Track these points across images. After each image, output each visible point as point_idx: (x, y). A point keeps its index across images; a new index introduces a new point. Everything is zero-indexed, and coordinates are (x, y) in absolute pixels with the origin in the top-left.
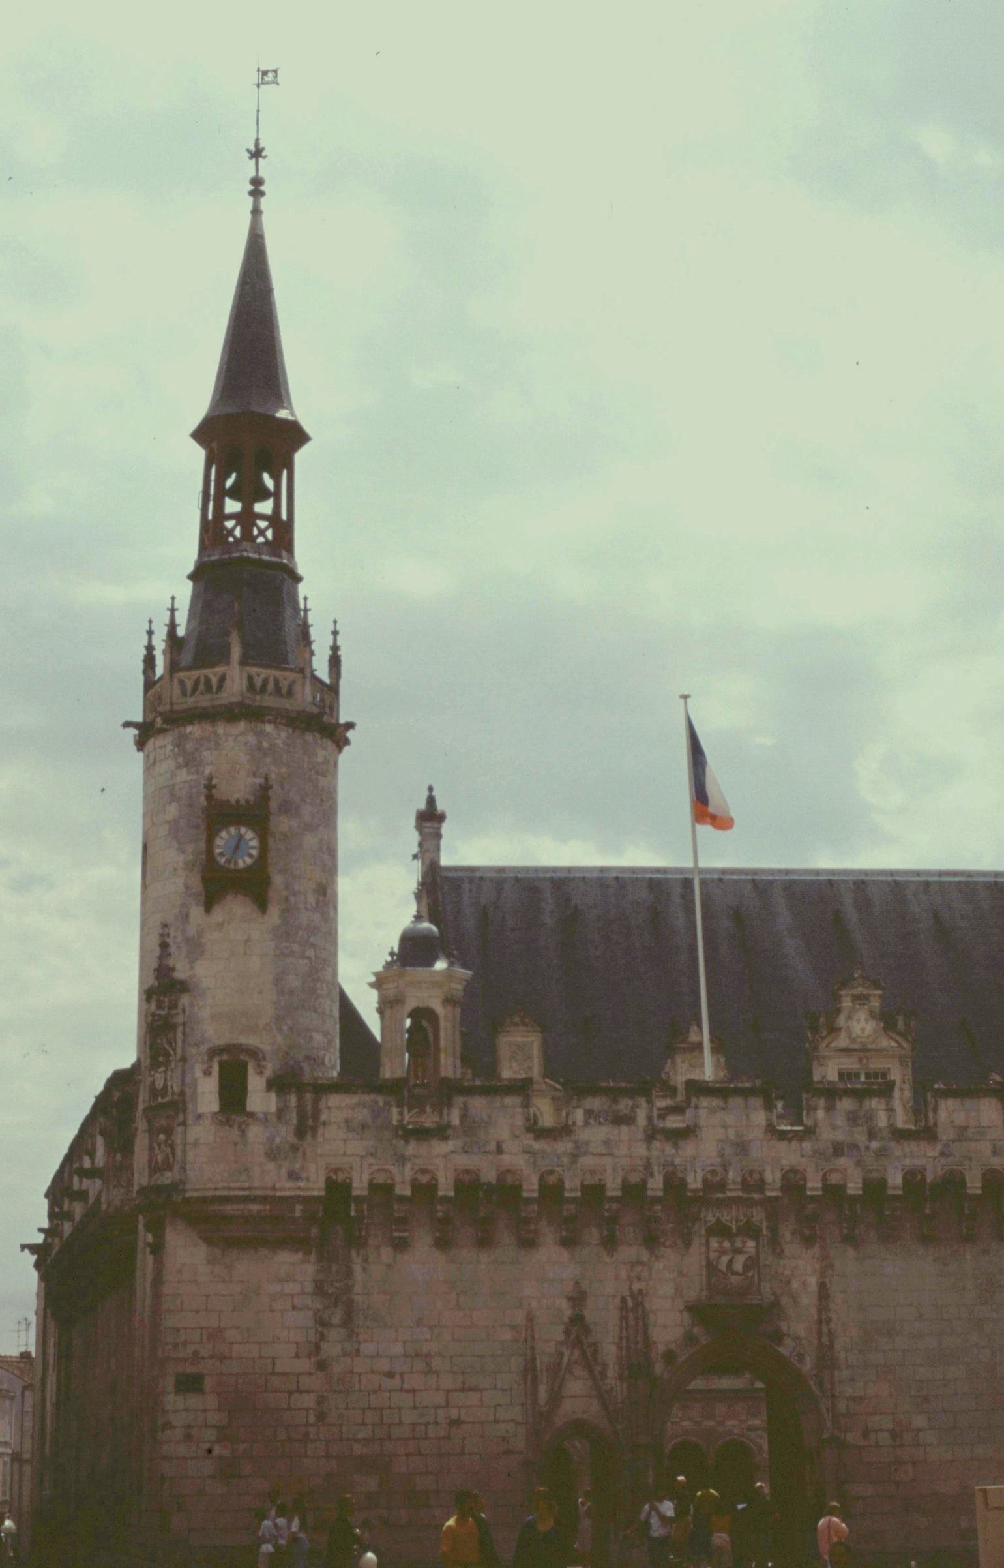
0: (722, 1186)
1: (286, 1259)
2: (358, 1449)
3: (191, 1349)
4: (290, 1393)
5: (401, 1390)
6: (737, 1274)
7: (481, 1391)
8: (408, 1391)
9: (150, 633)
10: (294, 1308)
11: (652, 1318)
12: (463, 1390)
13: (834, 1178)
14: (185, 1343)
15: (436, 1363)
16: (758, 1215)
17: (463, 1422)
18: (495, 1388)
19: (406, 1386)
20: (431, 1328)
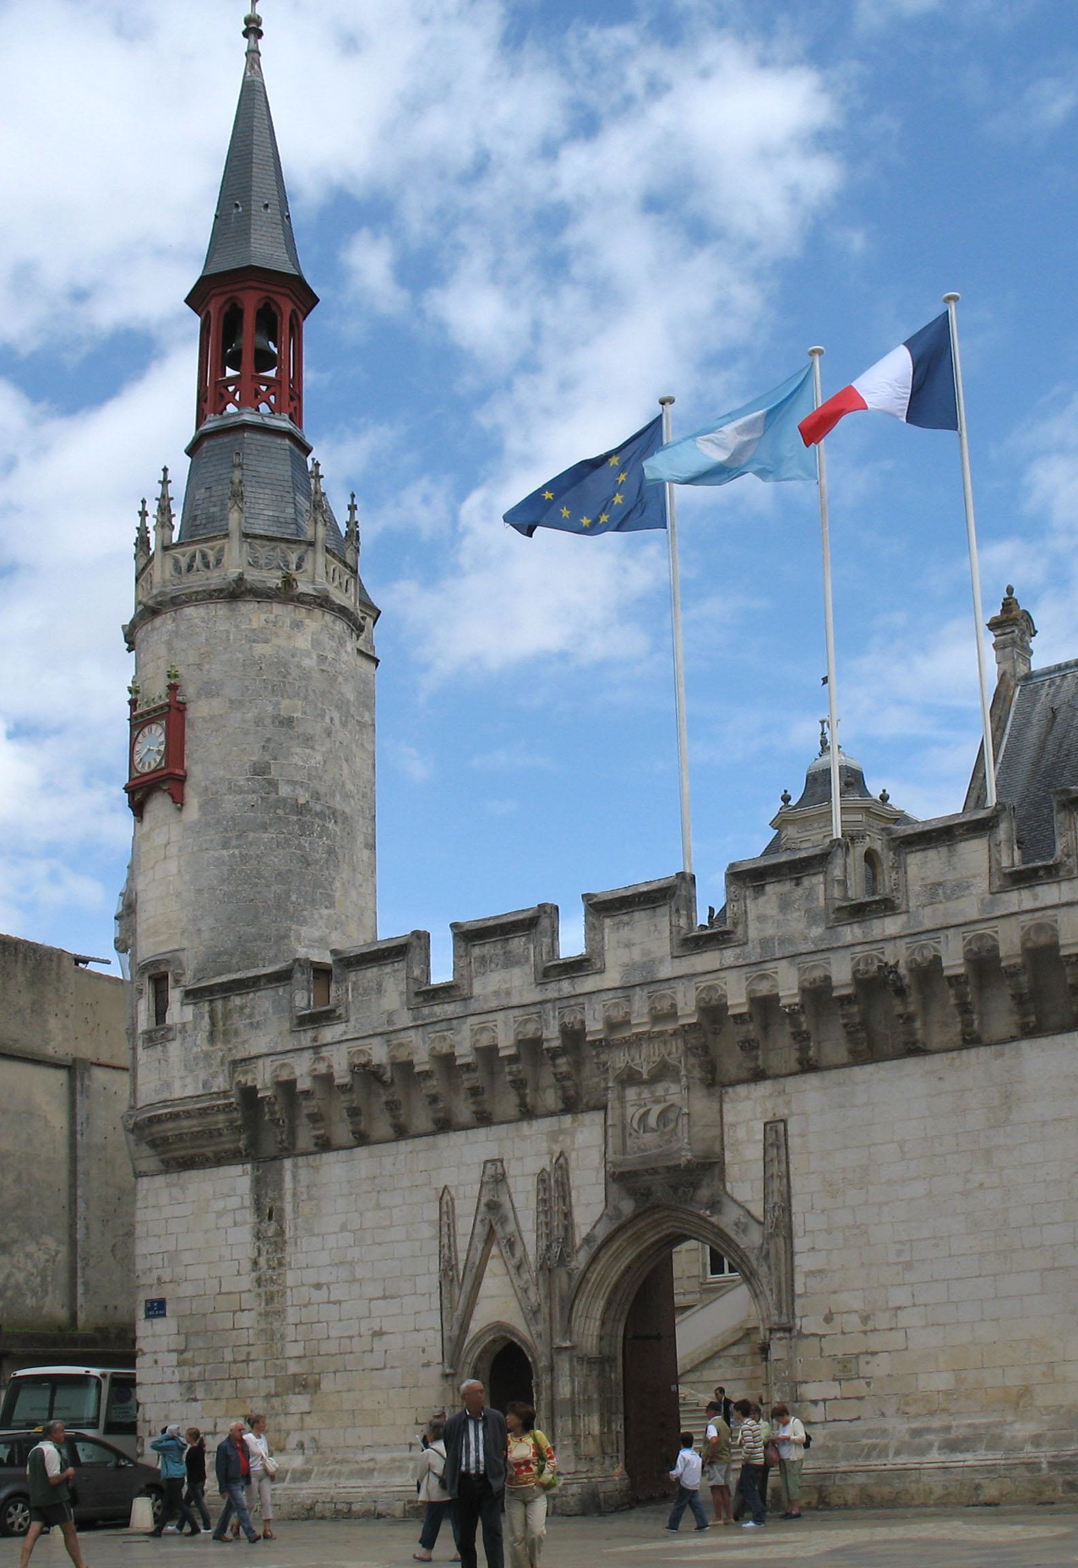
0: (626, 1023)
1: (236, 1170)
2: (293, 1368)
3: (155, 1274)
4: (235, 1312)
5: (329, 1302)
6: (654, 1130)
7: (401, 1297)
10: (235, 1224)
12: (384, 1298)
13: (763, 988)
14: (150, 1269)
15: (360, 1272)
16: (675, 1051)
17: (386, 1333)
18: (415, 1293)
19: (332, 1299)
20: (353, 1232)
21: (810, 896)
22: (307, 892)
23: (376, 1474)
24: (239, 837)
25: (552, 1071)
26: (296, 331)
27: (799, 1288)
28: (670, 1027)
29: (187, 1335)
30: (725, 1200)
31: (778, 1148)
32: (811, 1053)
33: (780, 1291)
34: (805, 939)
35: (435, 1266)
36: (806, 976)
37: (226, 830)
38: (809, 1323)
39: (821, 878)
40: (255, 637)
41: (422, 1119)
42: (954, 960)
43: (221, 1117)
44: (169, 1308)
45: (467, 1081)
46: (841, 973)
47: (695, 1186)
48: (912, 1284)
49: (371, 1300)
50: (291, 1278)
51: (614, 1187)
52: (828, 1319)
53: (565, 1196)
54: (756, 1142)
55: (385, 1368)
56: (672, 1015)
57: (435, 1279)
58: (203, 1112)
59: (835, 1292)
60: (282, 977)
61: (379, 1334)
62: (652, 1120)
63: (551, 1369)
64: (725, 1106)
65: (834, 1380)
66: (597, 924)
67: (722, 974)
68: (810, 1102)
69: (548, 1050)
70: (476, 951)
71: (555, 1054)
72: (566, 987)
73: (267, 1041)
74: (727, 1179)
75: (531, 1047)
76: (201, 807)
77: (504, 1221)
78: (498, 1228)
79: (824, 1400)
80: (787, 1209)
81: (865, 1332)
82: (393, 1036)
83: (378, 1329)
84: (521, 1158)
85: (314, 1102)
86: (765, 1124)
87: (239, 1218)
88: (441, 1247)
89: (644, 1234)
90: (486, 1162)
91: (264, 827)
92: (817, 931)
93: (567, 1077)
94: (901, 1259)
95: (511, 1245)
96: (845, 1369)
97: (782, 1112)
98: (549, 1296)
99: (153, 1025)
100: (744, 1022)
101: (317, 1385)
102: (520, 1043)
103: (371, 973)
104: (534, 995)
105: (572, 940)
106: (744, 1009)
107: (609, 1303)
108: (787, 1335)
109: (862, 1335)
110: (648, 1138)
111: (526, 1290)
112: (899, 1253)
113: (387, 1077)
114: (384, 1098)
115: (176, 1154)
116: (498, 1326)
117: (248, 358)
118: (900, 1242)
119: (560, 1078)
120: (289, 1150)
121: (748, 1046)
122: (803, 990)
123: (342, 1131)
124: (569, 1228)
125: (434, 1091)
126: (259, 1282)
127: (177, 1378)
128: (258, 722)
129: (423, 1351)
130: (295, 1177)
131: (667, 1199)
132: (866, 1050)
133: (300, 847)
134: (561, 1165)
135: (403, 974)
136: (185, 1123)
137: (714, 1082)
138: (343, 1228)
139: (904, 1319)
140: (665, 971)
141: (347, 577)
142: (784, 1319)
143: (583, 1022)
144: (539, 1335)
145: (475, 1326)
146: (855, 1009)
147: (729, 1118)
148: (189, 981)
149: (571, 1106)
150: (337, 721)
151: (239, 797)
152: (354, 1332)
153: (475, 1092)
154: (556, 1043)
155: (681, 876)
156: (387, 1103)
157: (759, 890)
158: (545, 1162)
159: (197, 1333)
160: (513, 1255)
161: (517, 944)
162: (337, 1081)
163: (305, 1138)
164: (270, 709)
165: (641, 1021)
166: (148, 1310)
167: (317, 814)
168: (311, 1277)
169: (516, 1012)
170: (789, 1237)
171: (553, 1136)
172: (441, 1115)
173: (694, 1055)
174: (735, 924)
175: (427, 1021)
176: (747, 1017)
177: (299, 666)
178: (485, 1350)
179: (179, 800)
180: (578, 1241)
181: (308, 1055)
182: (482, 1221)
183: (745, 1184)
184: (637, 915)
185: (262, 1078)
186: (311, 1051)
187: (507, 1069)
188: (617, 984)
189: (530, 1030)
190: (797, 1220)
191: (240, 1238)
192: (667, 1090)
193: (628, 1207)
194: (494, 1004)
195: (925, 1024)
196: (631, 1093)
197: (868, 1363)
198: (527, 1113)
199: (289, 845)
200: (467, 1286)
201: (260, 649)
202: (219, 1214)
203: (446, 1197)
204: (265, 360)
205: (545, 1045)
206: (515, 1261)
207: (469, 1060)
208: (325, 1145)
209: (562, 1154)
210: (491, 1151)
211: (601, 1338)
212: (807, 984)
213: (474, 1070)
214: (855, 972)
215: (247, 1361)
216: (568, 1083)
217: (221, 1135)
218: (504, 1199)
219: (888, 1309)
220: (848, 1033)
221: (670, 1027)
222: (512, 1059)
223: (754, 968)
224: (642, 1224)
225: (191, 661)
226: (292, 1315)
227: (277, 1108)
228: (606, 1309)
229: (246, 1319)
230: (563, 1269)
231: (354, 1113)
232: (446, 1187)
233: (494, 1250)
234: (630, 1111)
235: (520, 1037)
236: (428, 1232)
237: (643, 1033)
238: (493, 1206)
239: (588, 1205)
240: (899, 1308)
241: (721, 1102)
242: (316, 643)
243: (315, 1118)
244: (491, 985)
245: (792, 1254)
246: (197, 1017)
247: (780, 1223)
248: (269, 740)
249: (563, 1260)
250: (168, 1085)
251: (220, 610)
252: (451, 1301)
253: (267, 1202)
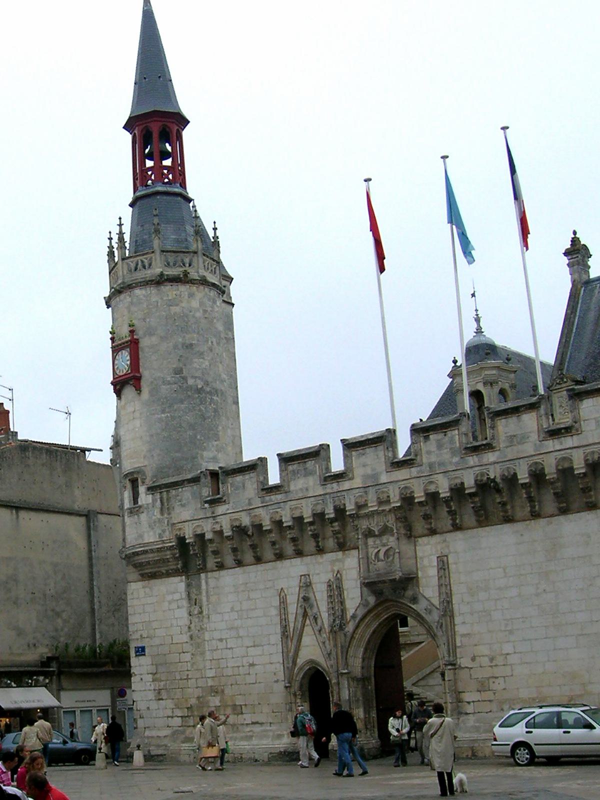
0: (365, 505)
1: (176, 579)
3: (140, 633)
4: (180, 653)
5: (227, 648)
6: (382, 561)
8: (229, 649)
9: (110, 239)
10: (178, 607)
11: (345, 592)
12: (254, 646)
13: (432, 489)
16: (391, 521)
20: (237, 611)
21: (452, 441)
22: (205, 433)
23: (254, 738)
24: (170, 407)
25: (329, 529)
26: (180, 138)
27: (458, 644)
28: (387, 508)
29: (156, 665)
30: (420, 597)
31: (444, 569)
32: (457, 521)
33: (448, 646)
34: (451, 463)
35: (278, 630)
36: (452, 482)
37: (163, 404)
38: (464, 662)
39: (456, 432)
40: (171, 303)
41: (268, 553)
42: (523, 477)
43: (168, 552)
44: (147, 650)
45: (289, 535)
46: (469, 481)
47: (405, 589)
48: (514, 642)
49: (248, 647)
50: (207, 636)
51: (365, 589)
52: (473, 659)
53: (341, 594)
54: (435, 566)
55: (256, 683)
56: (388, 502)
57: (279, 636)
58: (159, 550)
59: (476, 645)
60: (195, 480)
61: (252, 665)
62: (381, 555)
63: (338, 684)
64: (417, 548)
65: (478, 691)
66: (349, 455)
67: (411, 481)
68: (458, 545)
69: (328, 519)
70: (290, 468)
71: (332, 521)
72: (335, 486)
73: (189, 515)
74: (420, 585)
75: (320, 517)
76: (150, 392)
77: (311, 606)
78: (308, 610)
79: (473, 702)
80: (449, 602)
81: (491, 666)
82: (251, 511)
83: (251, 662)
84: (318, 574)
85: (214, 545)
86: (438, 557)
87: (180, 604)
88: (281, 620)
89: (381, 614)
90: (301, 576)
91: (182, 402)
92: (456, 459)
93: (339, 533)
94: (508, 629)
95: (316, 619)
96: (483, 687)
97: (446, 552)
98: (336, 646)
99: (133, 506)
100: (424, 506)
101: (223, 691)
102: (314, 515)
103: (239, 478)
104: (320, 491)
105: (337, 464)
106: (423, 499)
107: (366, 649)
108: (453, 667)
109: (490, 668)
110: (380, 564)
111: (324, 643)
112: (506, 625)
113: (250, 533)
114: (249, 543)
115: (147, 571)
116: (311, 661)
117: (156, 155)
119: (335, 533)
120: (204, 569)
121: (426, 517)
122: (451, 490)
123: (229, 560)
124: (343, 611)
125: (273, 540)
126: (191, 637)
127: (152, 687)
128: (176, 347)
129: (275, 674)
130: (207, 583)
131: (392, 595)
132: (484, 519)
133: (200, 410)
134: (339, 579)
135: (254, 480)
136: (151, 555)
137: (410, 535)
138: (232, 609)
139: (512, 659)
140: (384, 478)
141: (214, 266)
142: (451, 659)
143: (345, 505)
144: (332, 666)
145: (300, 661)
146: (477, 499)
147: (419, 554)
148: (149, 482)
149: (342, 546)
150: (215, 343)
151: (168, 386)
152: (240, 665)
153: (294, 540)
154: (332, 516)
155: (388, 430)
156: (251, 546)
157: (427, 438)
158: (330, 576)
159: (161, 664)
160: (317, 624)
161: (310, 464)
162: (226, 534)
163: (211, 562)
164: (180, 340)
165: (373, 506)
166: (136, 652)
167: (208, 393)
168: (217, 635)
169: (312, 499)
170: (452, 616)
171: (333, 562)
172: (278, 551)
173: (401, 522)
174: (416, 455)
175: (268, 504)
177: (194, 316)
178: (305, 674)
179: (138, 389)
180: (349, 617)
181: (211, 520)
182: (301, 606)
183: (429, 588)
184: (368, 450)
185: (189, 533)
186: (212, 519)
187: (309, 528)
188: (361, 486)
189: (319, 509)
190: (456, 607)
191: (182, 614)
192: (388, 540)
193: (372, 600)
194: (300, 495)
195: (512, 507)
196: (370, 541)
197: (494, 682)
198: (321, 551)
199: (195, 410)
200: (295, 641)
201: (175, 309)
202: (170, 602)
203: (283, 594)
204: (165, 155)
205: (327, 517)
206: (318, 628)
207: (290, 524)
208: (221, 566)
209: (338, 572)
210: (303, 570)
211: (363, 668)
212: (453, 486)
213: (293, 529)
214: (476, 481)
215: (187, 679)
216: (339, 536)
217: (169, 562)
218: (311, 595)
219: (502, 654)
220: (475, 511)
221: (387, 508)
222: (311, 524)
223: (427, 478)
224: (380, 609)
225: (140, 317)
226: (208, 656)
227: (196, 548)
228: (364, 653)
229: (187, 657)
230: (342, 632)
231: (235, 550)
232: (282, 589)
233: (308, 622)
234: (370, 550)
235: (314, 512)
236: (274, 612)
237: (374, 511)
238: (306, 599)
240: (508, 654)
241: (415, 546)
242: (201, 304)
243: (216, 553)
244: (297, 485)
245: (454, 625)
246: (154, 501)
247: (447, 611)
248: (181, 356)
249: (341, 628)
250: (141, 536)
251: (152, 291)
252: (287, 648)
253: (193, 597)
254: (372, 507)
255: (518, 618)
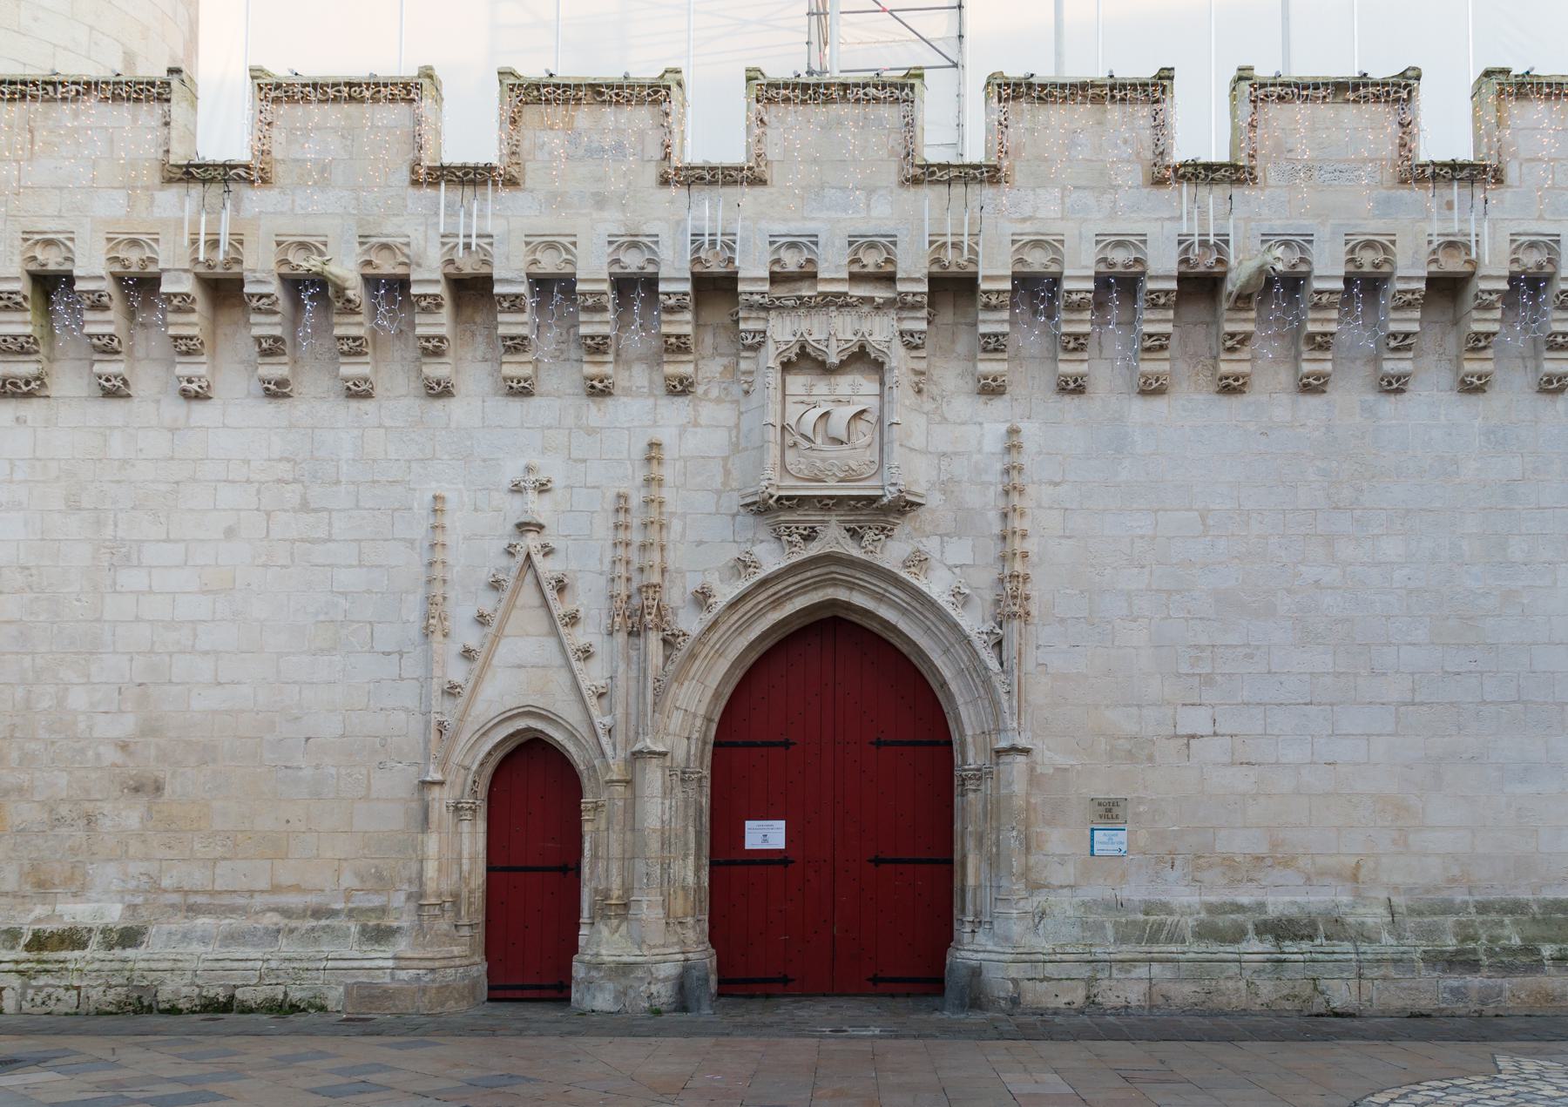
28: (880, 293)
94: (1197, 671)
118: (1196, 647)
176: (1006, 298)
196: (797, 383)
219: (1176, 736)
234: (793, 412)
237: (838, 295)
239: (700, 543)
240: (1193, 737)
254: (826, 280)
255: (1236, 646)
